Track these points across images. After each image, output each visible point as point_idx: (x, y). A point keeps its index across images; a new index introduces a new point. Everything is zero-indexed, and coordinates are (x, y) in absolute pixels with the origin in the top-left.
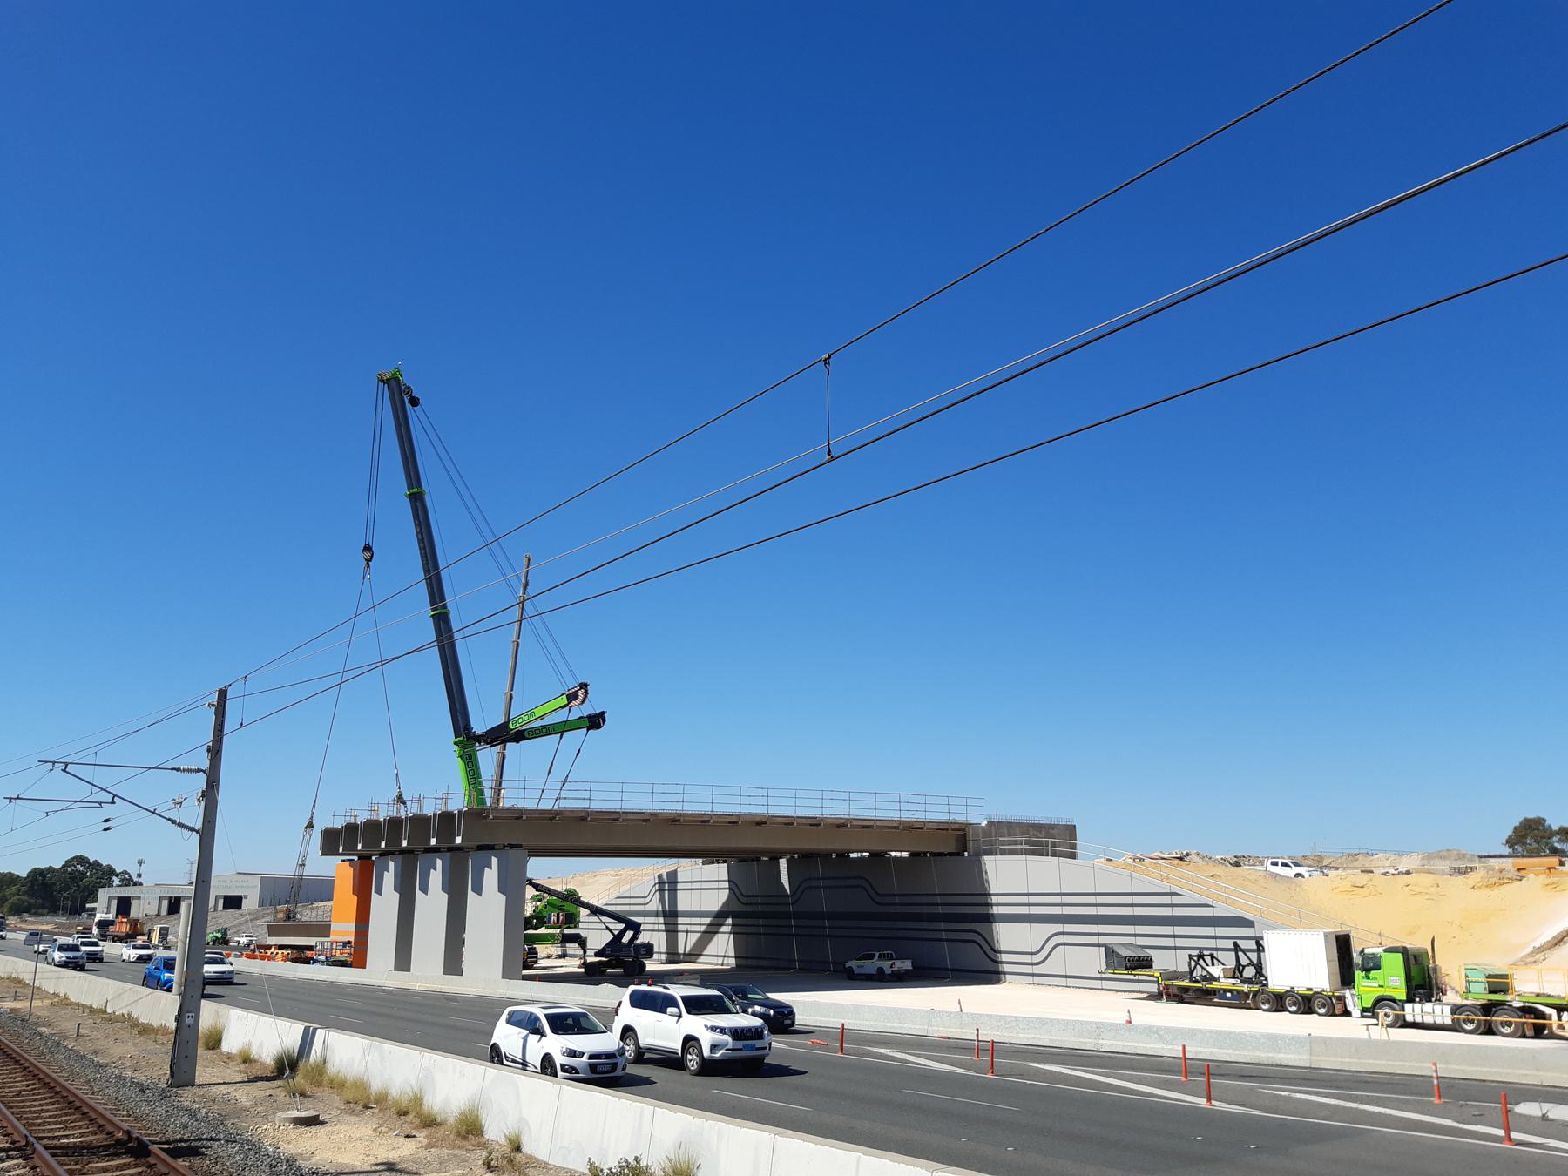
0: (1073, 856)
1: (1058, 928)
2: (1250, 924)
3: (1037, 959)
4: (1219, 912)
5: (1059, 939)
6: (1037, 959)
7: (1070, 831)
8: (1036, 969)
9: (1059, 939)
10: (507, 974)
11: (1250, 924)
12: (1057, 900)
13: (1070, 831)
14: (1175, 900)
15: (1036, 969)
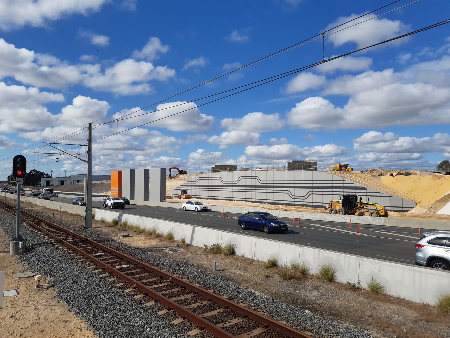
0: (316, 170)
1: (311, 190)
2: (365, 189)
3: (304, 198)
4: (358, 185)
5: (311, 193)
6: (304, 198)
7: (315, 163)
8: (304, 201)
9: (311, 193)
10: (161, 201)
11: (365, 189)
12: (302, 182)
13: (315, 163)
14: (345, 182)
15: (304, 201)
